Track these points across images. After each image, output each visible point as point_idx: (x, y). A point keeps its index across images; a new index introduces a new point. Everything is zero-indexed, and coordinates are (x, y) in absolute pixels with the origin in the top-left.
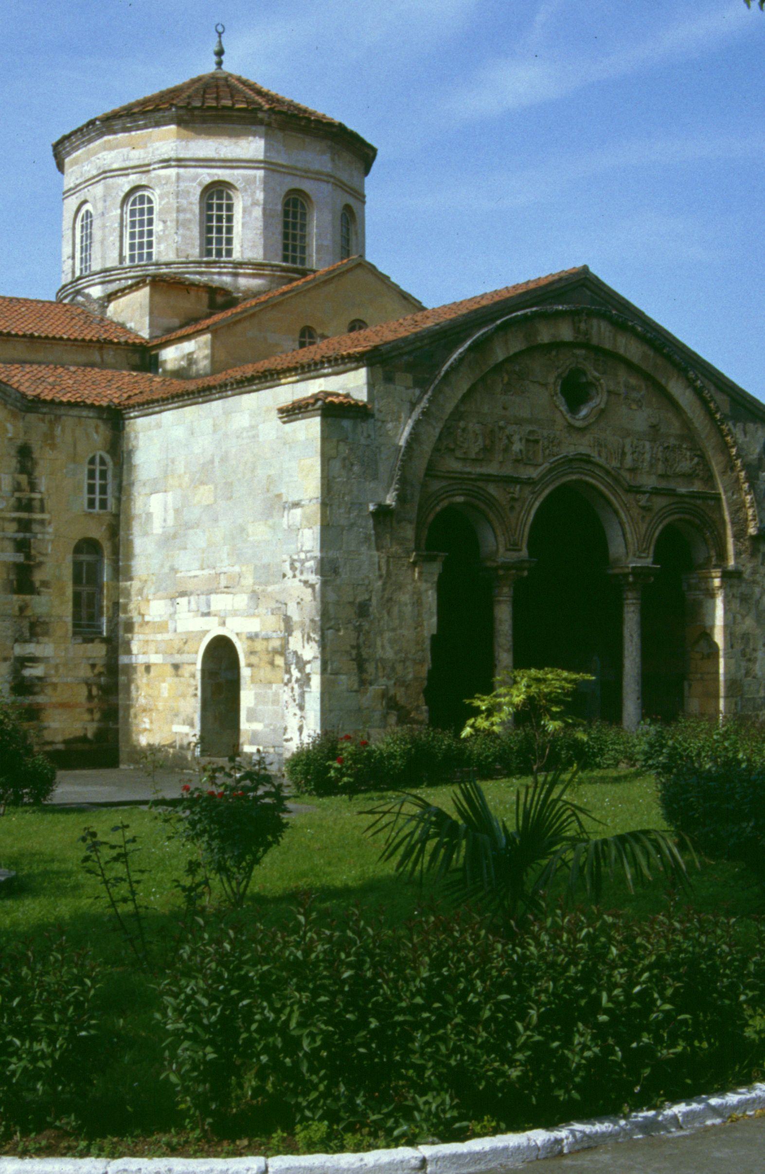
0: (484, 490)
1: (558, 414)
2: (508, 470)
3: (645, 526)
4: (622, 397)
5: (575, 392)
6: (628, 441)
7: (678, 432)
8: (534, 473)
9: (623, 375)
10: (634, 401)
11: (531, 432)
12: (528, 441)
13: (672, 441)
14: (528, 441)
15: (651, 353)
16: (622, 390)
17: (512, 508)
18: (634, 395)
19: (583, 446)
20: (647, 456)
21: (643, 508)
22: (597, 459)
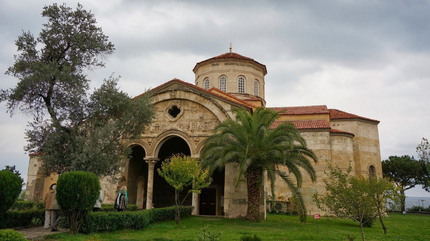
1: (166, 118)
2: (149, 135)
3: (196, 146)
6: (191, 122)
8: (156, 135)
9: (190, 104)
11: (157, 124)
13: (209, 121)
15: (199, 97)
16: (190, 109)
18: (195, 109)
19: (175, 126)
20: (198, 126)
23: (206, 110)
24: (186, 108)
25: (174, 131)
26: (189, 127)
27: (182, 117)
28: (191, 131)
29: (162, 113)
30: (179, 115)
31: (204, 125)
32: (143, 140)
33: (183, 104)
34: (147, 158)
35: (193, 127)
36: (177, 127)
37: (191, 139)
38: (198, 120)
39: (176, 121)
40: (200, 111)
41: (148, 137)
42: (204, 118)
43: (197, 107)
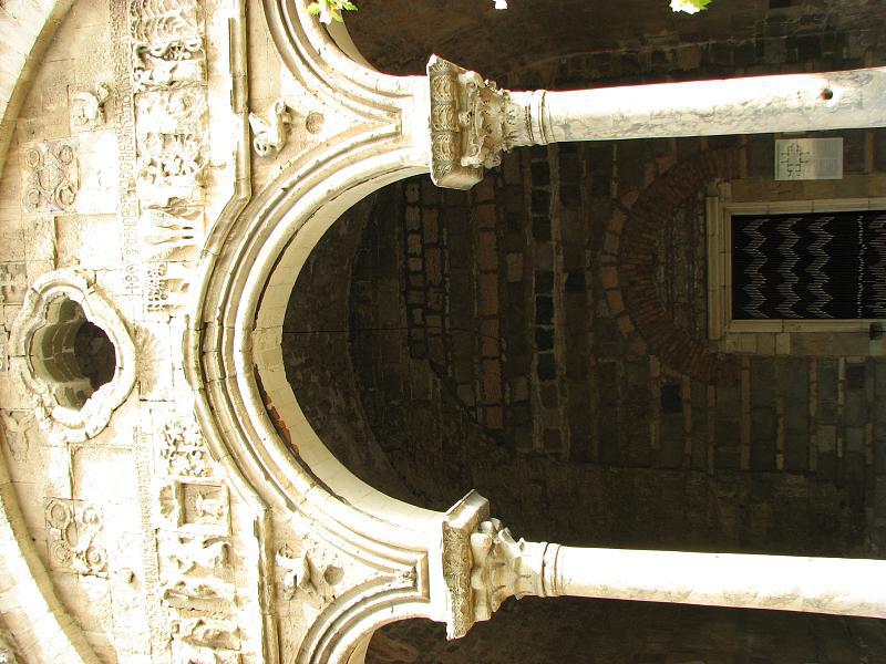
0: (302, 651)
4: (59, 213)
5: (80, 354)
7: (108, 13)
8: (249, 510)
10: (63, 174)
11: (166, 510)
12: (184, 520)
13: (129, 41)
14: (184, 520)
16: (45, 214)
17: (331, 575)
18: (51, 175)
19: (170, 341)
21: (287, 128)
22: (190, 303)
23: (50, 70)
24: (44, 248)
25: (212, 343)
26: (173, 206)
27: (102, 281)
28: (204, 182)
29: (85, 463)
30: (97, 313)
31: (161, 71)
32: (294, 635)
33: (19, 282)
34: (441, 607)
35: (172, 167)
36: (179, 325)
37: (269, 173)
38: (122, 137)
39: (133, 332)
40: (62, 121)
41: (270, 588)
42: (109, 76)
43: (35, 154)
